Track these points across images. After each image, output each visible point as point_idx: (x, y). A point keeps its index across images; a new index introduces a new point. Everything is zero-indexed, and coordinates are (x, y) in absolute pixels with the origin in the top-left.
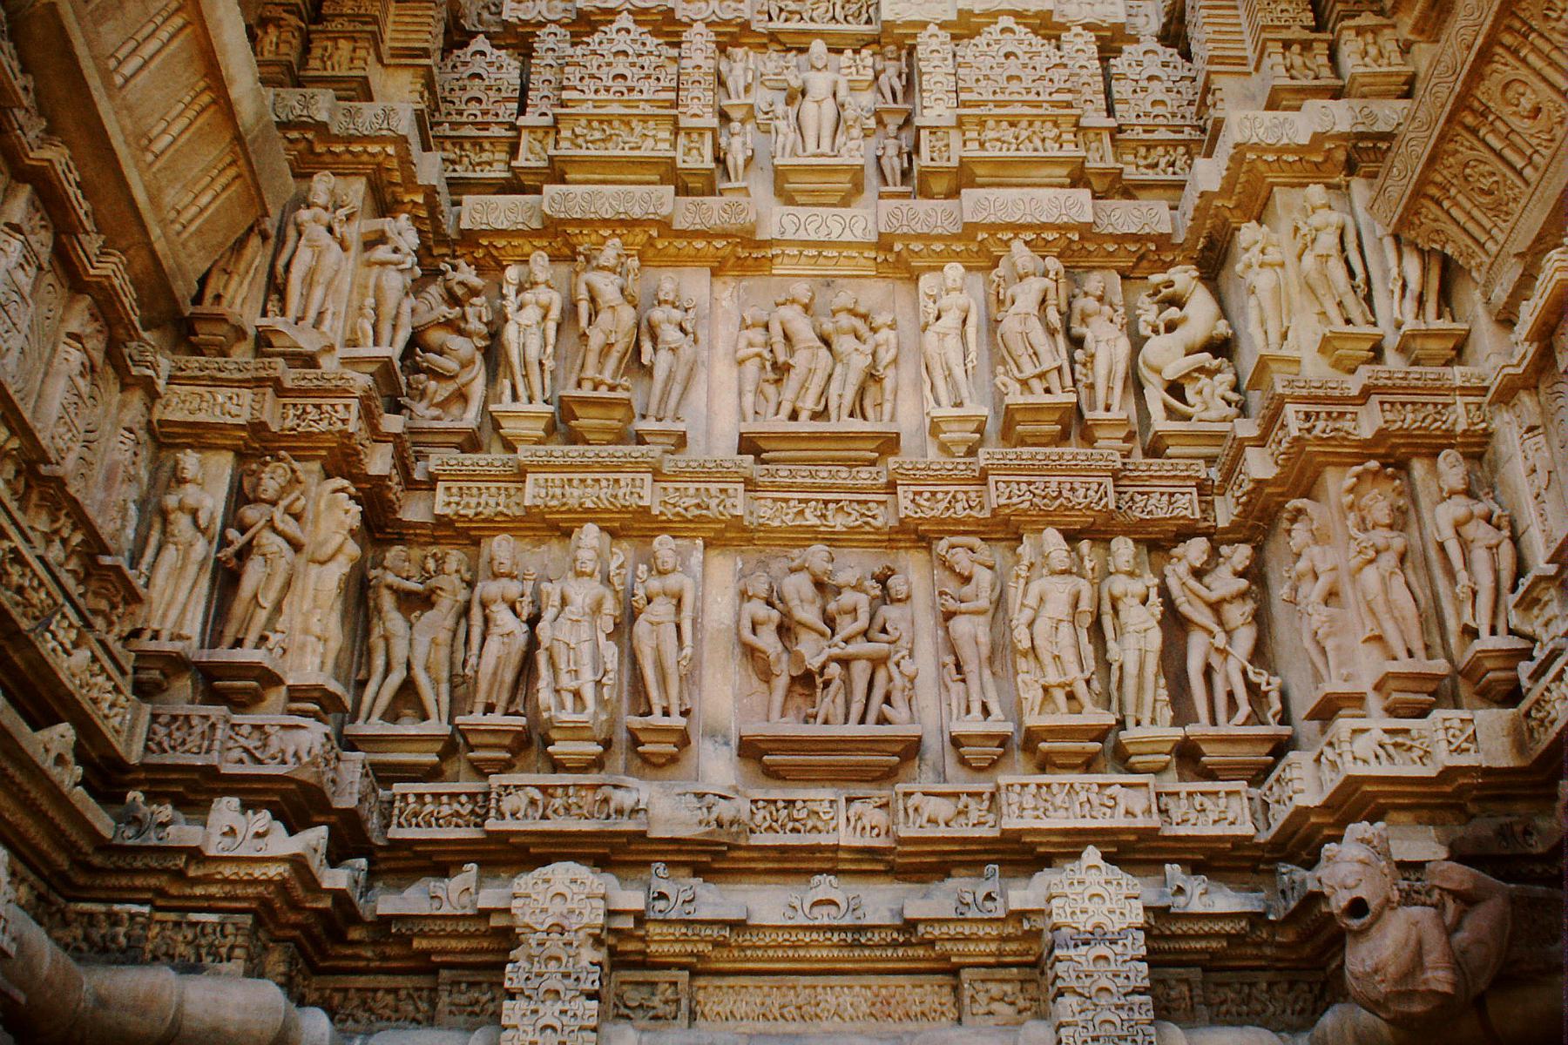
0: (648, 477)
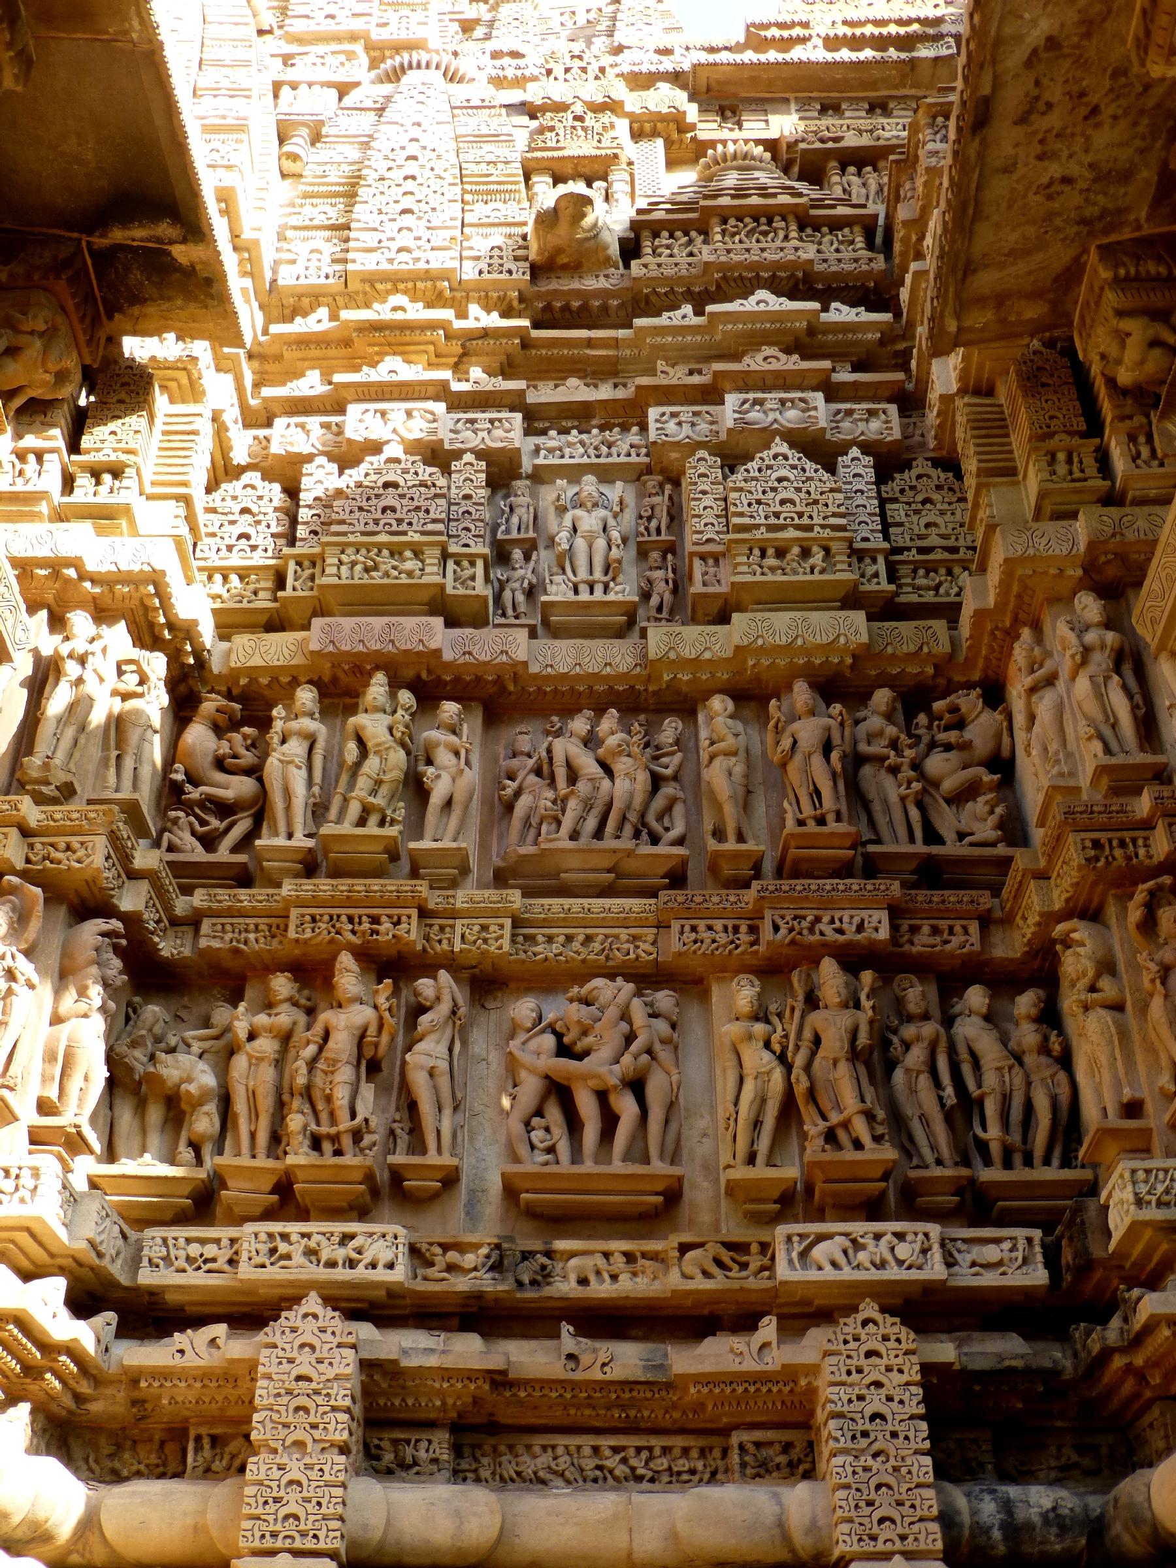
0: (414, 913)
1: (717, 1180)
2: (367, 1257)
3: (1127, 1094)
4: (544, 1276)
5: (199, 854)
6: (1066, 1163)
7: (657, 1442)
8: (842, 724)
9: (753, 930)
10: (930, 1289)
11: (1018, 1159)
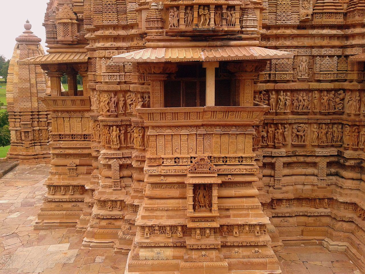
3: (348, 143)
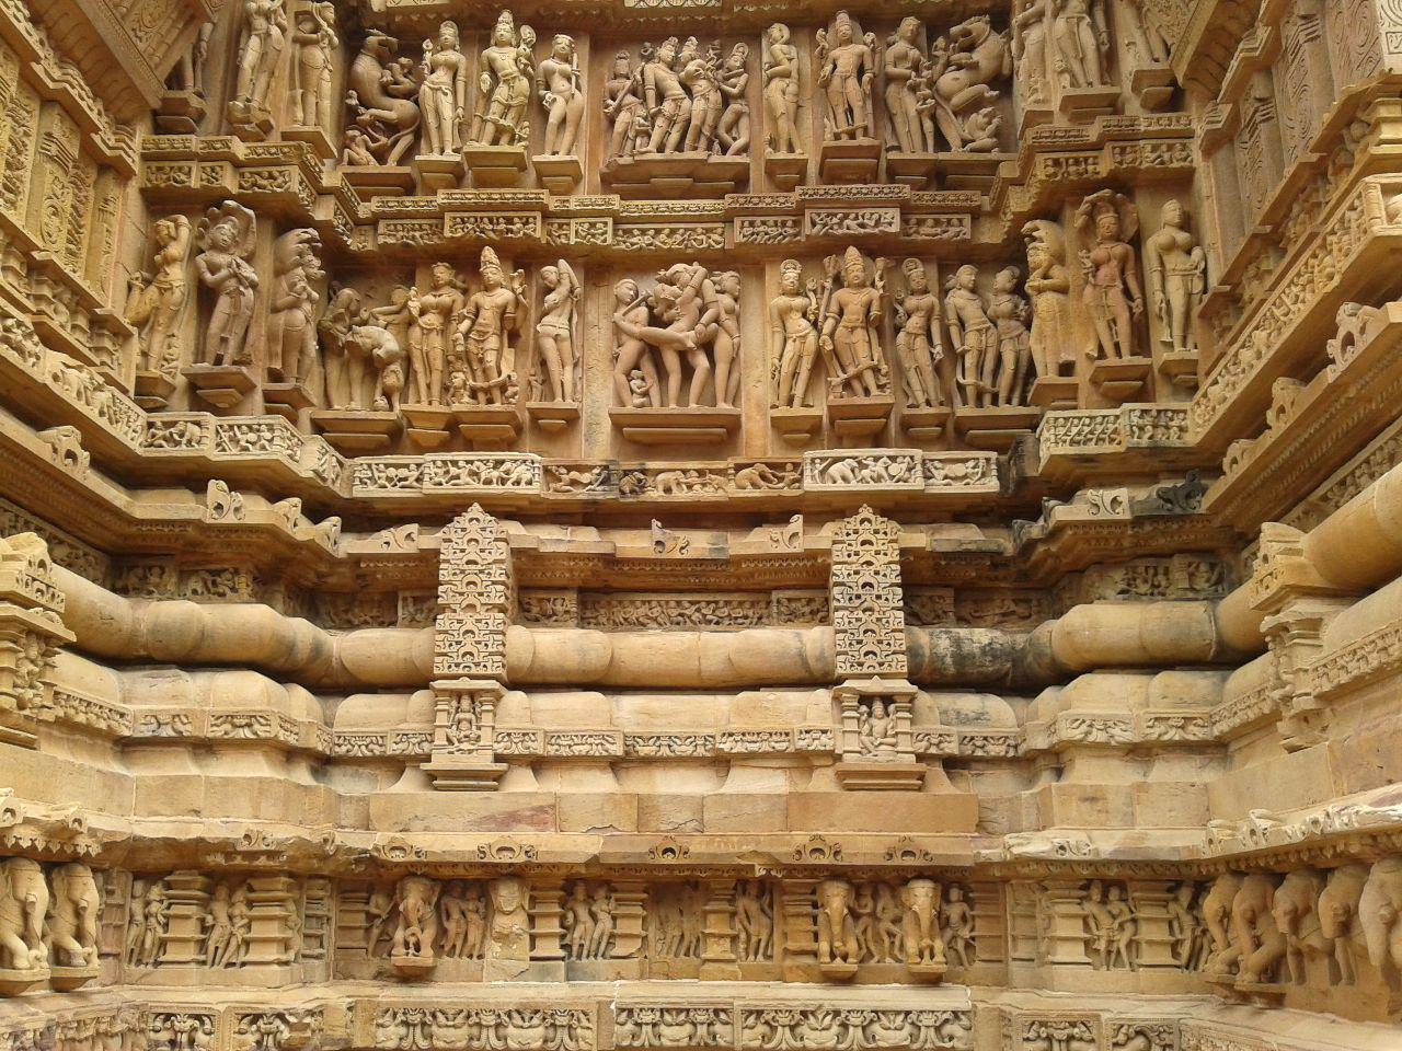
0: (538, 215)
1: (766, 414)
2: (514, 477)
3: (1065, 357)
4: (641, 486)
5: (373, 167)
6: (1023, 402)
7: (718, 597)
8: (873, 50)
9: (796, 224)
10: (913, 496)
11: (987, 399)
